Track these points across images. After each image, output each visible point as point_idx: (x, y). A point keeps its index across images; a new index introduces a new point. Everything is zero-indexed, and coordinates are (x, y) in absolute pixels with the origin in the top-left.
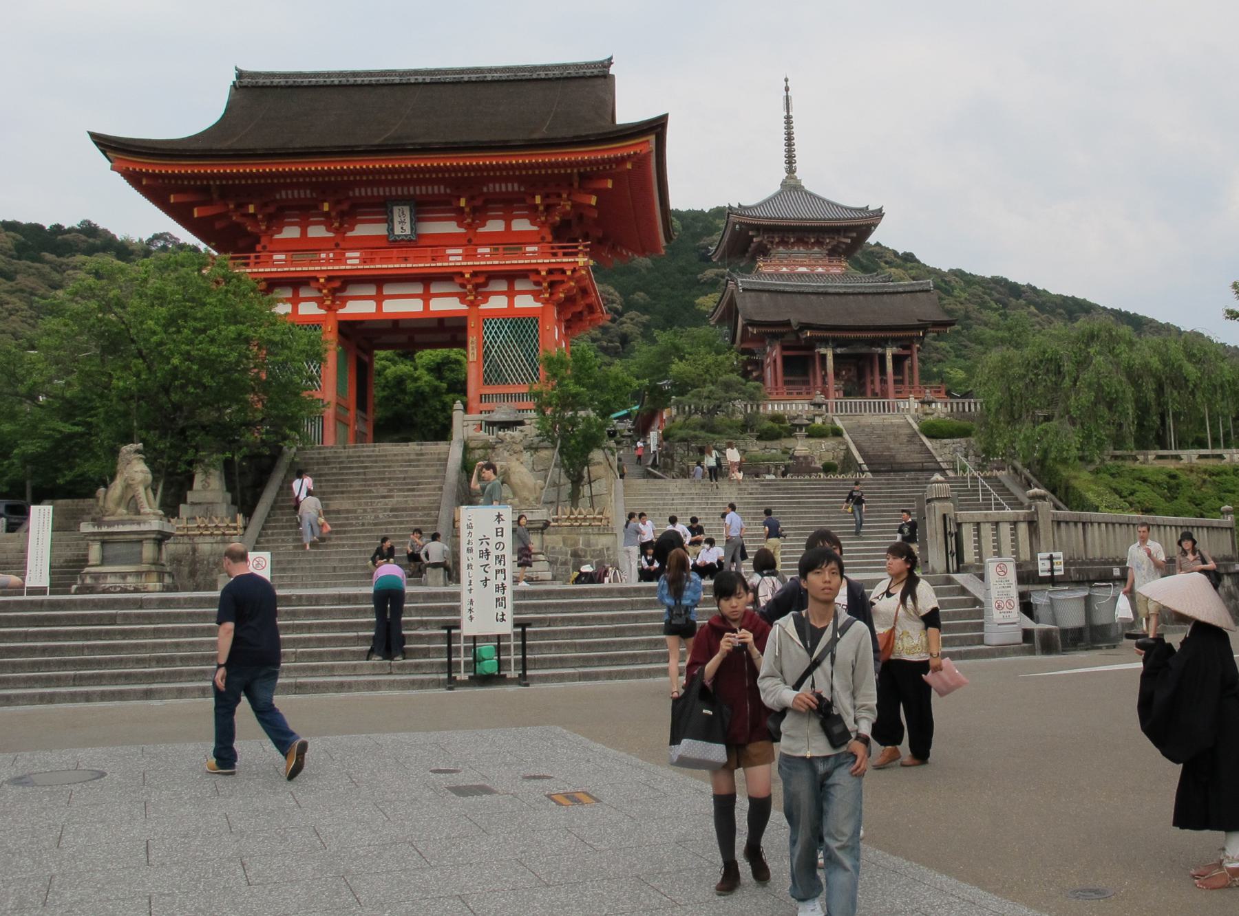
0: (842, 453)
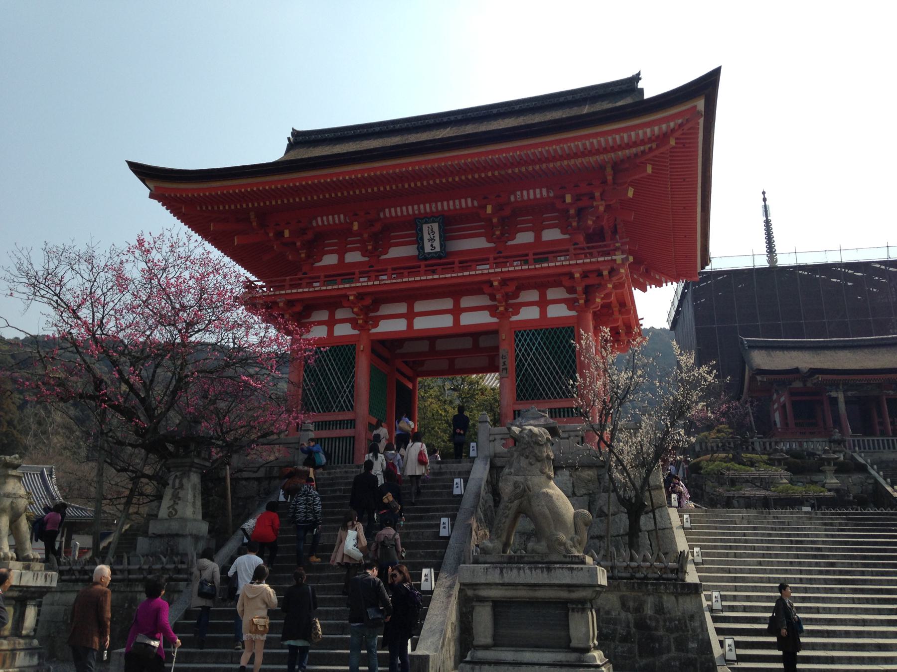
0: (870, 487)
